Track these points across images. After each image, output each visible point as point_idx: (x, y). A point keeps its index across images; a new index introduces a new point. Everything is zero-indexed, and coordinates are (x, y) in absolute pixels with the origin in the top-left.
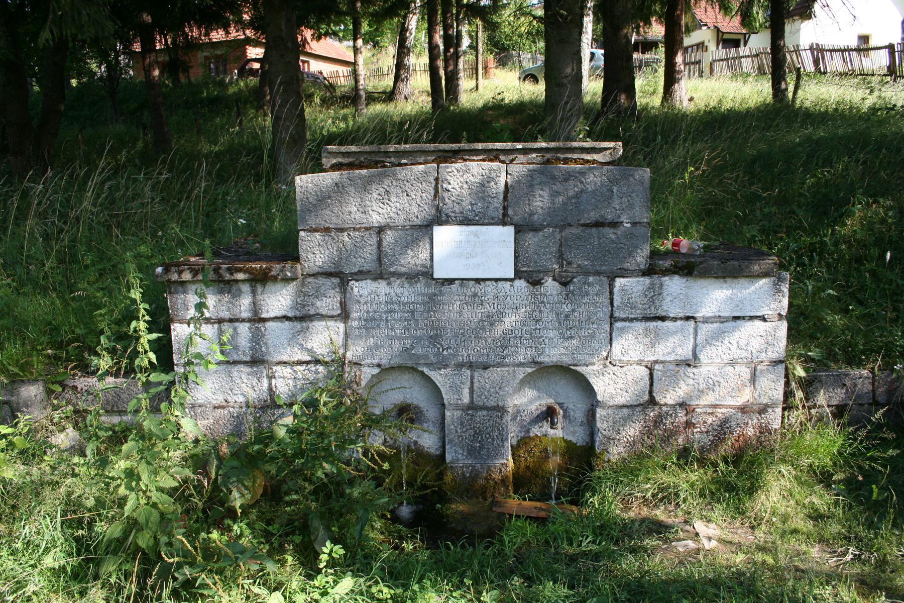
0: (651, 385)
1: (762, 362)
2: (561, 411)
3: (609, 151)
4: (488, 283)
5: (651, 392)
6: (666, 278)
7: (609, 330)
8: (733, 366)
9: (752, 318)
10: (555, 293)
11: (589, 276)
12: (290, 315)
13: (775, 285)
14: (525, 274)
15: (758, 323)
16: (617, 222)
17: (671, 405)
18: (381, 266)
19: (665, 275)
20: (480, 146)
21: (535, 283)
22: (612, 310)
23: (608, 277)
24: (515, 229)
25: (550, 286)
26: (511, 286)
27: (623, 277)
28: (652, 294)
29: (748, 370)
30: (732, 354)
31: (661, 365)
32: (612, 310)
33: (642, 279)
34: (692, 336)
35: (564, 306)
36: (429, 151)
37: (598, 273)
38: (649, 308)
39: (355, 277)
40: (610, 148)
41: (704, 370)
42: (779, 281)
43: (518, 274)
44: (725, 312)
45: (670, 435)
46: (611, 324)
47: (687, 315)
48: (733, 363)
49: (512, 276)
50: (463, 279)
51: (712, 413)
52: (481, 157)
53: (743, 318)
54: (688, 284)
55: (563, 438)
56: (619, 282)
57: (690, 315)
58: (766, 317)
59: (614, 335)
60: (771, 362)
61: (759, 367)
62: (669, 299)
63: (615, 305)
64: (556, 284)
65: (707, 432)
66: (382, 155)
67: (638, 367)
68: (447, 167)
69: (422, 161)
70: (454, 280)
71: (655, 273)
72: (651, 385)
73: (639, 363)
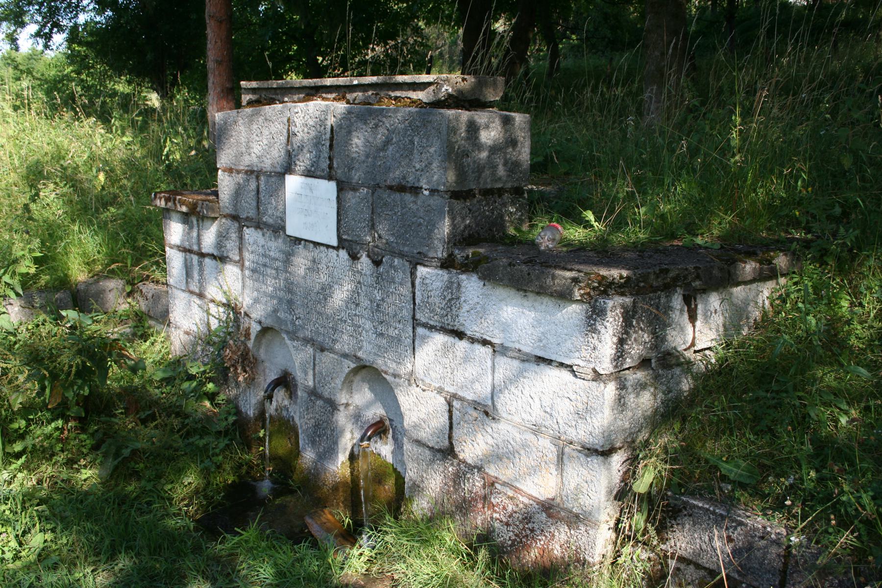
0: (451, 427)
1: (571, 443)
2: (391, 430)
3: (432, 88)
4: (322, 248)
5: (450, 437)
6: (463, 277)
7: (412, 335)
8: (536, 435)
9: (562, 365)
10: (368, 273)
11: (395, 257)
12: (215, 254)
13: (589, 318)
14: (347, 244)
15: (565, 375)
16: (417, 188)
17: (470, 465)
18: (259, 215)
19: (463, 272)
20: (328, 81)
21: (354, 257)
22: (414, 309)
23: (410, 262)
24: (338, 185)
25: (365, 261)
26: (338, 256)
27: (425, 266)
28: (449, 296)
29: (553, 448)
30: (534, 415)
31: (460, 403)
32: (414, 309)
33: (440, 272)
34: (490, 371)
35: (376, 291)
36: (292, 88)
37: (401, 255)
38: (447, 315)
39: (246, 223)
40: (430, 84)
41: (502, 426)
42: (593, 312)
43: (342, 244)
44: (525, 345)
45: (464, 507)
46: (414, 328)
47: (485, 337)
48: (536, 430)
49: (335, 243)
50: (306, 241)
51: (511, 498)
52: (334, 95)
53: (549, 362)
54: (489, 289)
55: (393, 465)
56: (422, 271)
57: (488, 338)
58: (575, 368)
59: (416, 343)
60: (583, 447)
61: (567, 450)
62: (466, 307)
63: (417, 302)
64: (370, 262)
65: (507, 524)
66: (273, 91)
67: (438, 396)
68: (295, 107)
69: (296, 99)
70: (302, 239)
71: (455, 268)
72: (451, 427)
73: (440, 391)
